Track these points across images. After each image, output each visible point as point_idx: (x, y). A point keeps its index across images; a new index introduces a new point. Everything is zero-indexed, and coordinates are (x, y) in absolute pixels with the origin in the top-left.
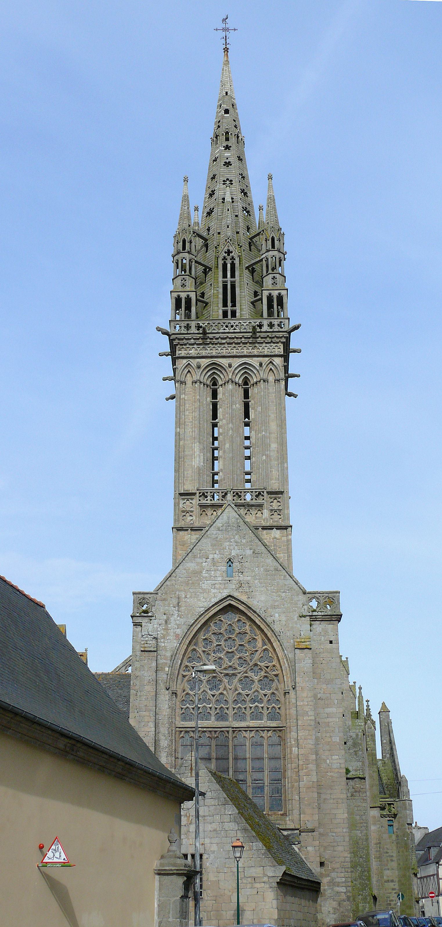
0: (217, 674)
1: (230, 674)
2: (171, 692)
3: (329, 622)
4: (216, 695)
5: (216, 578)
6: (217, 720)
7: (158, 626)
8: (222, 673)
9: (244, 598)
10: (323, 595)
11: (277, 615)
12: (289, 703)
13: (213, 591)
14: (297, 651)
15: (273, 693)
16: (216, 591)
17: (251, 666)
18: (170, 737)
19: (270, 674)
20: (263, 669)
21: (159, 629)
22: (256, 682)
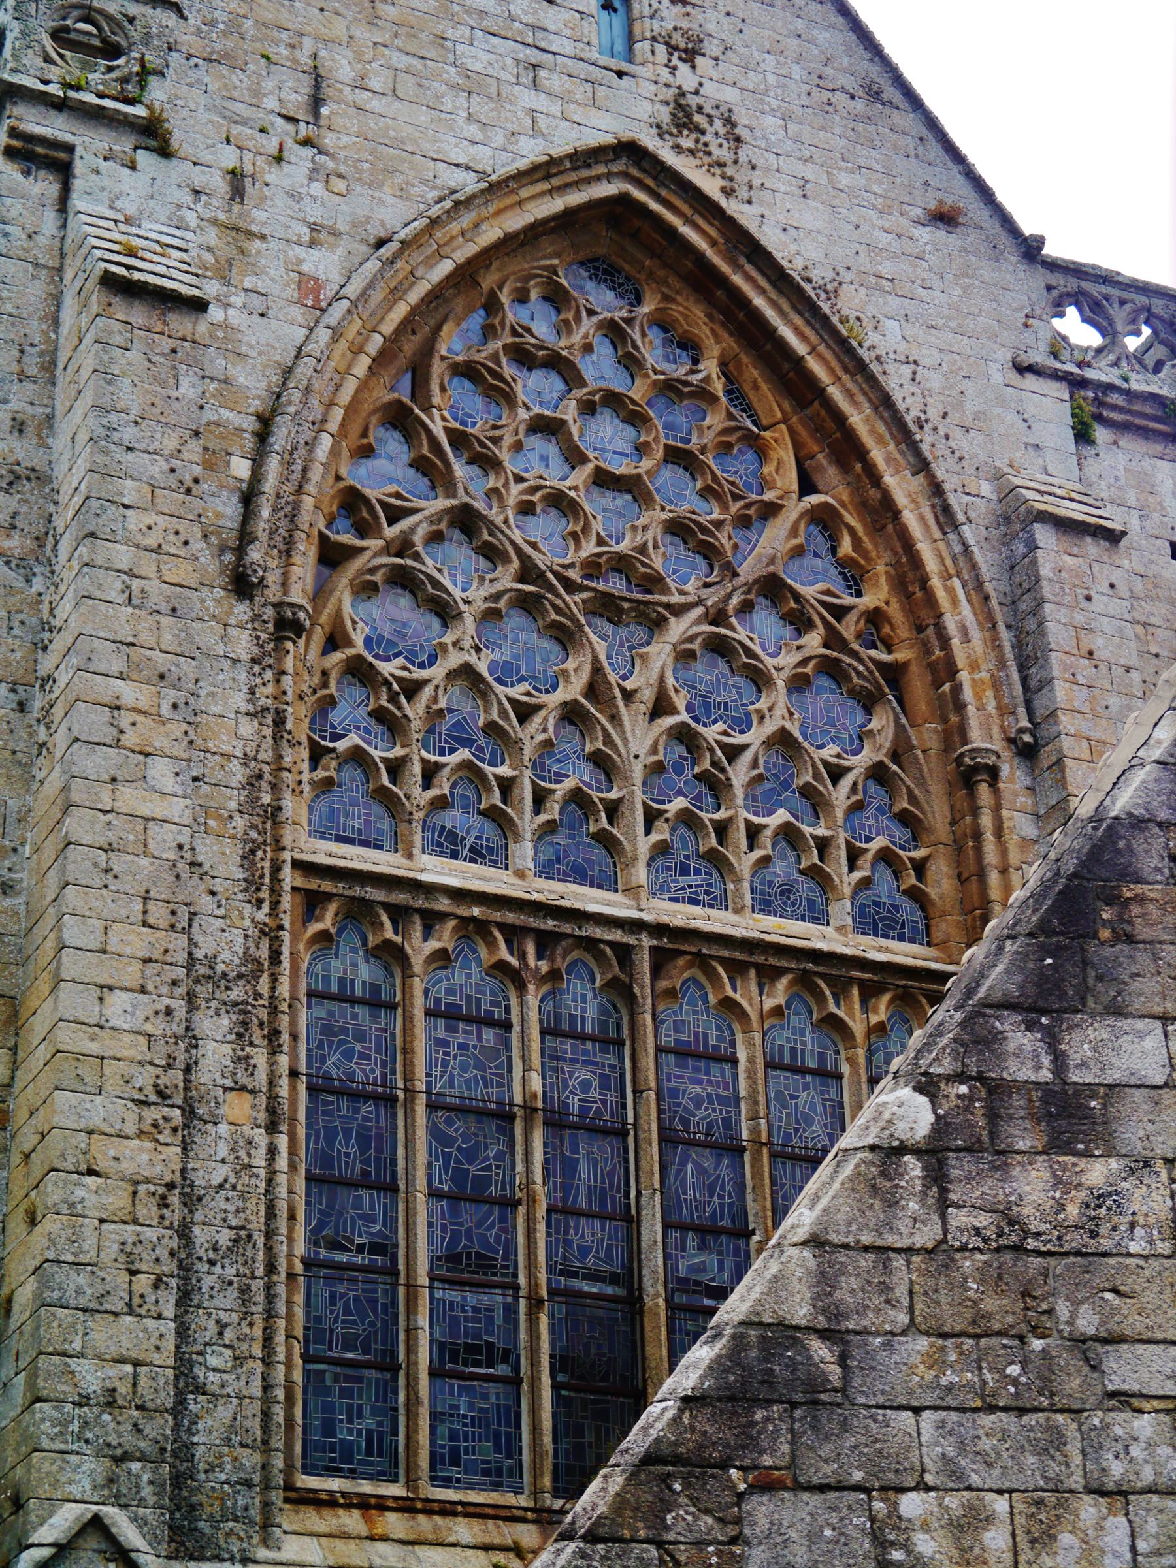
0: (552, 589)
1: (626, 605)
2: (269, 613)
3: (1158, 448)
4: (543, 713)
5: (540, 34)
6: (545, 870)
7: (188, 199)
8: (570, 586)
9: (710, 186)
10: (1125, 295)
11: (891, 326)
12: (999, 832)
13: (528, 98)
14: (1043, 534)
15: (877, 773)
16: (541, 102)
17: (749, 587)
18: (266, 908)
19: (855, 655)
20: (818, 622)
21: (191, 218)
22: (780, 684)
